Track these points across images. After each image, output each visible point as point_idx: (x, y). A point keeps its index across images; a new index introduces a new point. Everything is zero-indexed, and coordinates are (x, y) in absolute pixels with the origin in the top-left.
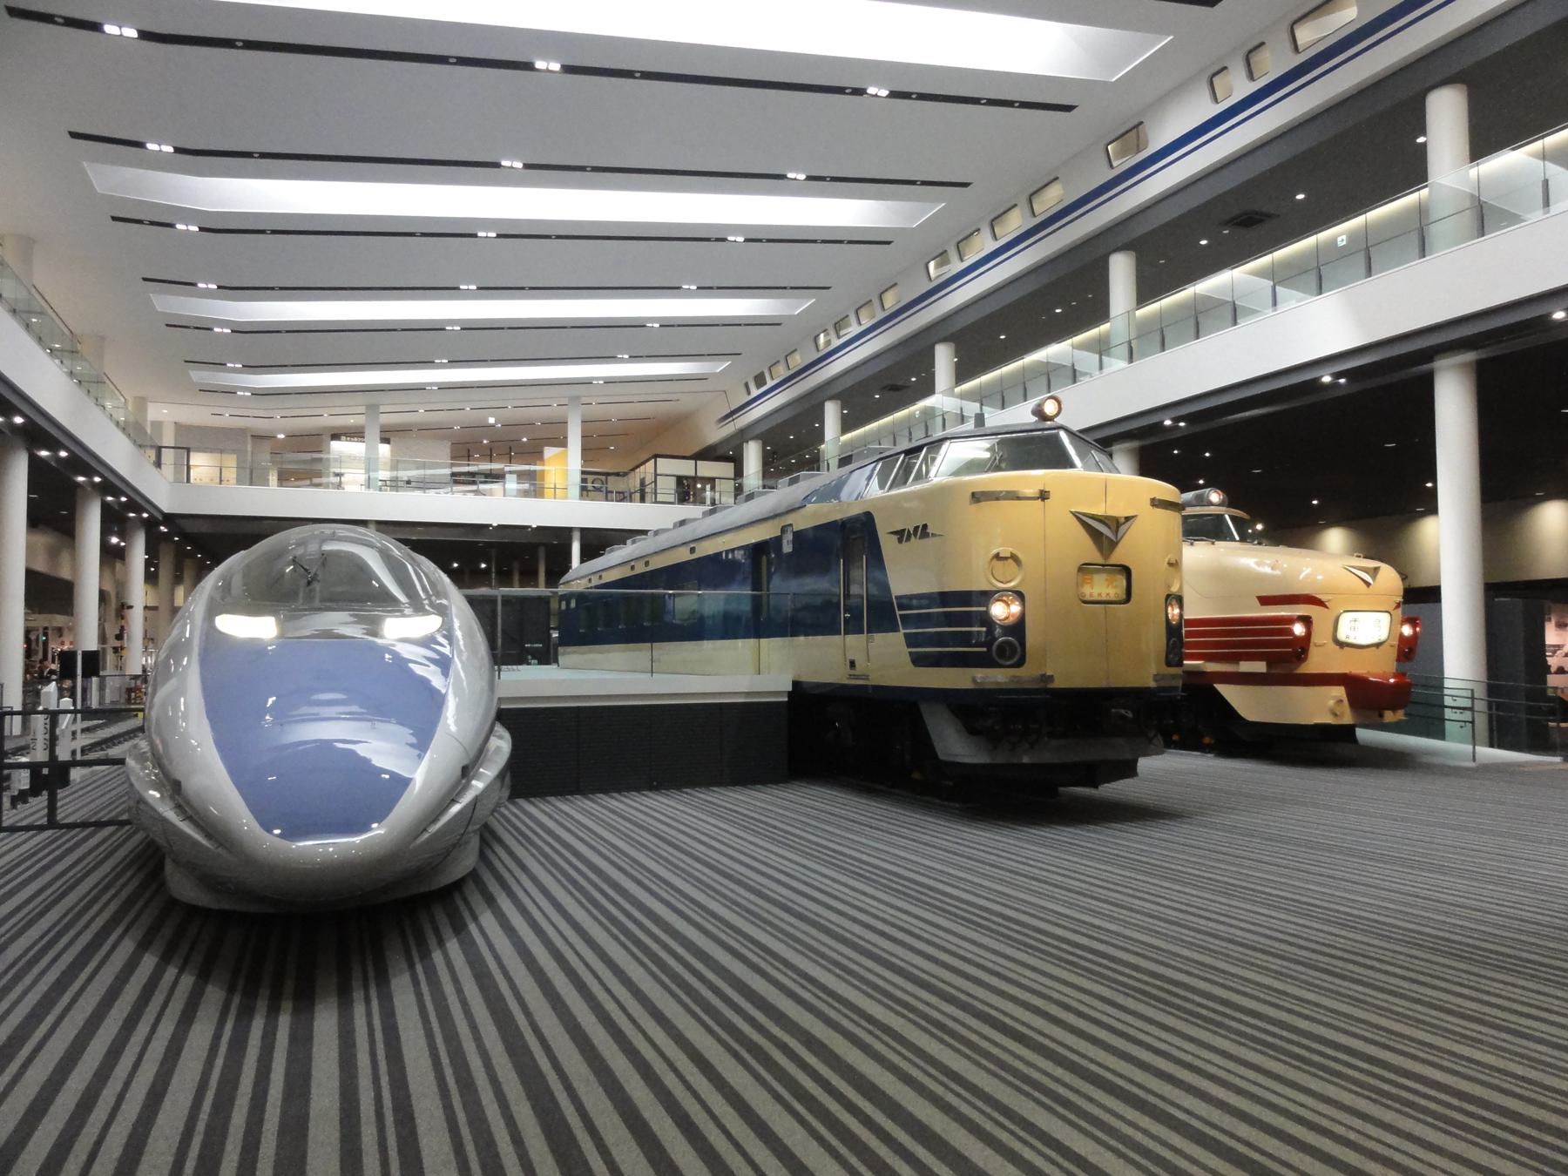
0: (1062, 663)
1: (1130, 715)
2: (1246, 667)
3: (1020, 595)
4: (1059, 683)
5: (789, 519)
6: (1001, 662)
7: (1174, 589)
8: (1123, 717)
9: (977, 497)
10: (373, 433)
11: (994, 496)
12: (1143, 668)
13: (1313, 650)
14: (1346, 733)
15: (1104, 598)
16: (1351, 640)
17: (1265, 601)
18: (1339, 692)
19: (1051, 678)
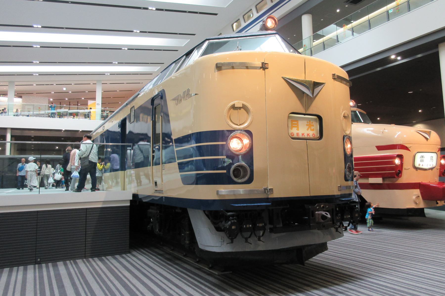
0: (278, 180)
1: (329, 216)
2: (372, 180)
3: (249, 133)
4: (276, 194)
5: (133, 104)
6: (235, 179)
7: (348, 132)
8: (324, 217)
9: (219, 67)
10: (11, 93)
11: (232, 66)
12: (328, 182)
13: (404, 172)
14: (420, 212)
15: (306, 136)
16: (421, 167)
17: (380, 148)
18: (417, 192)
19: (271, 190)
